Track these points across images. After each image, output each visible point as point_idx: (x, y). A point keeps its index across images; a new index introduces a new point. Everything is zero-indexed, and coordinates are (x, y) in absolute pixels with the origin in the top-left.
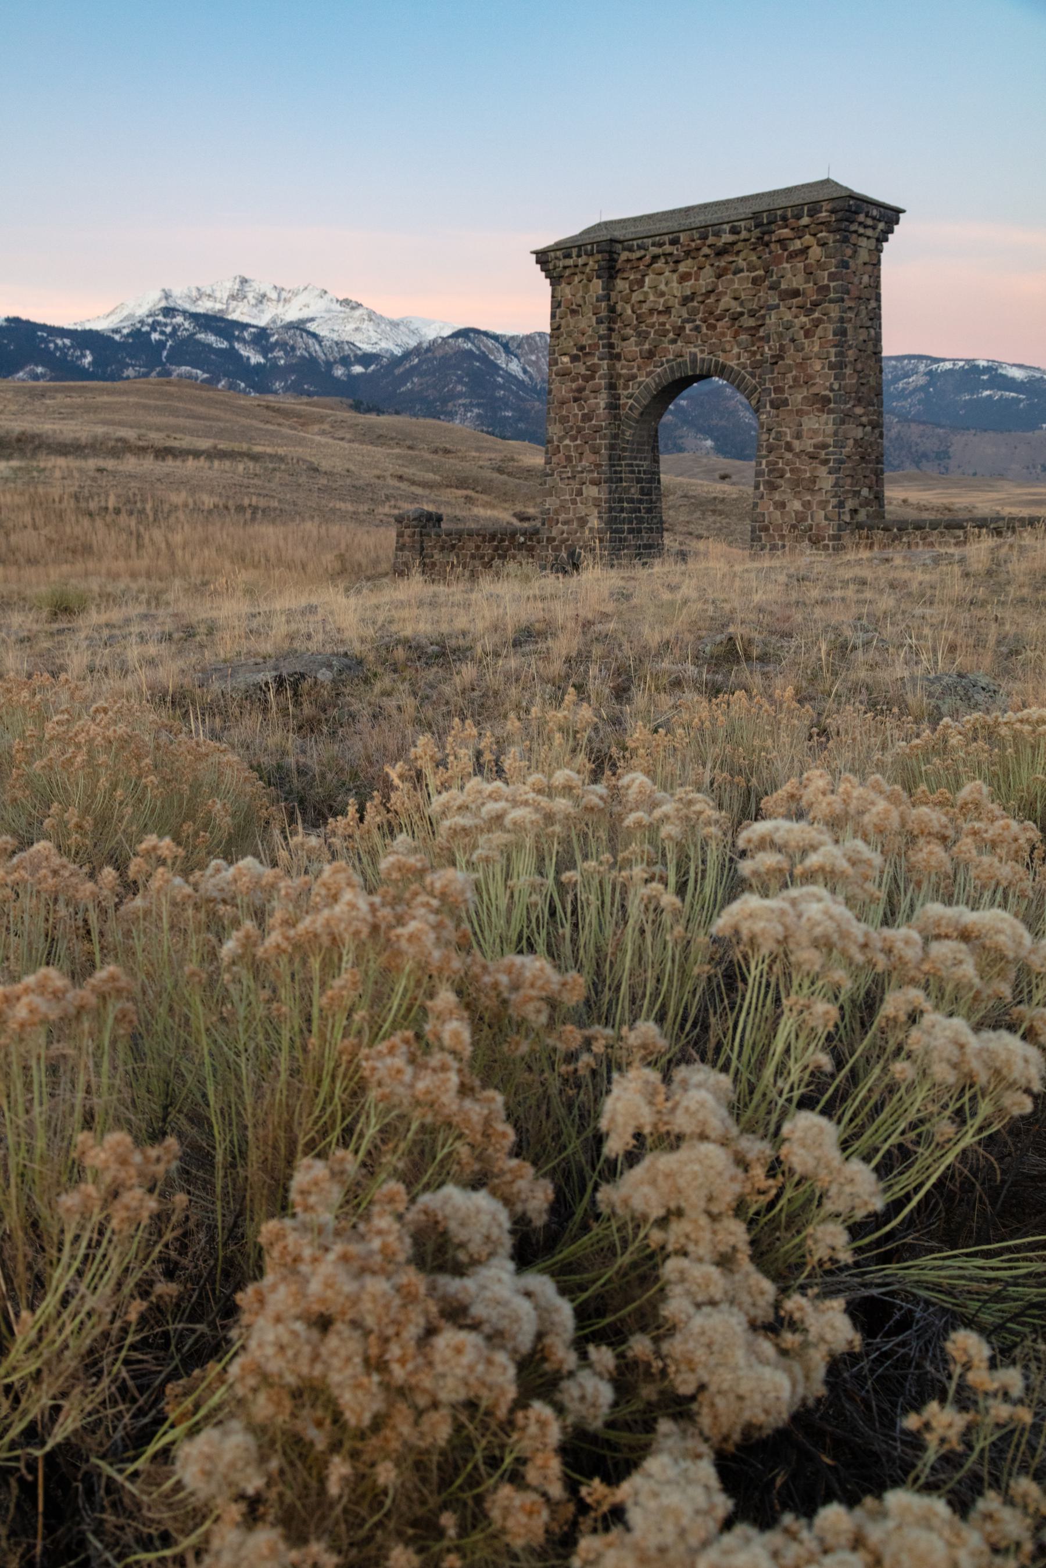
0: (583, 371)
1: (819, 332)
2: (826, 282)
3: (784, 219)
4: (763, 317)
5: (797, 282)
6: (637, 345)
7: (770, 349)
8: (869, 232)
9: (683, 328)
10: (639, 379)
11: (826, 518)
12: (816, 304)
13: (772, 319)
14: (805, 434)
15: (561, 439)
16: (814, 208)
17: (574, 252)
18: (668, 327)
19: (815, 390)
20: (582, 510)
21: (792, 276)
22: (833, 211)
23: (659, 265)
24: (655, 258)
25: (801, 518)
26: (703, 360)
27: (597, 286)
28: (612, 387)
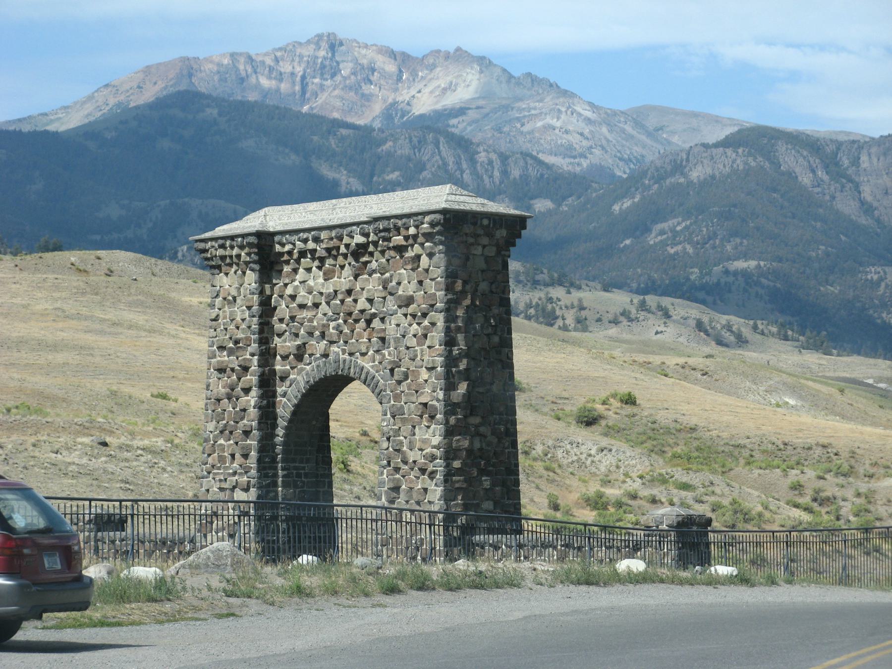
2: (433, 291)
7: (390, 354)
8: (485, 241)
10: (292, 377)
18: (315, 323)
19: (423, 399)
24: (303, 254)
26: (344, 361)
27: (251, 278)
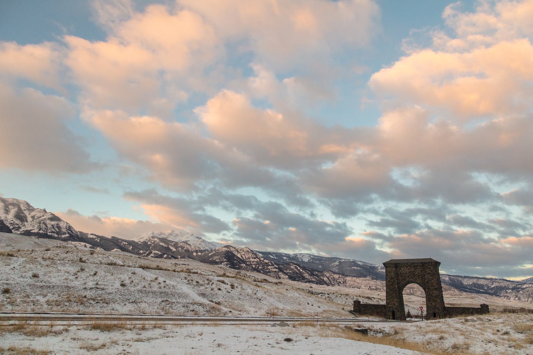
0: (392, 281)
1: (434, 279)
3: (427, 263)
4: (424, 276)
5: (430, 272)
6: (401, 278)
9: (409, 276)
11: (439, 306)
12: (433, 275)
13: (426, 276)
14: (434, 293)
15: (389, 291)
16: (432, 263)
17: (390, 264)
19: (435, 287)
20: (395, 303)
21: (429, 271)
22: (434, 263)
23: (405, 267)
24: (404, 266)
25: (435, 306)
27: (394, 269)
28: (398, 284)
